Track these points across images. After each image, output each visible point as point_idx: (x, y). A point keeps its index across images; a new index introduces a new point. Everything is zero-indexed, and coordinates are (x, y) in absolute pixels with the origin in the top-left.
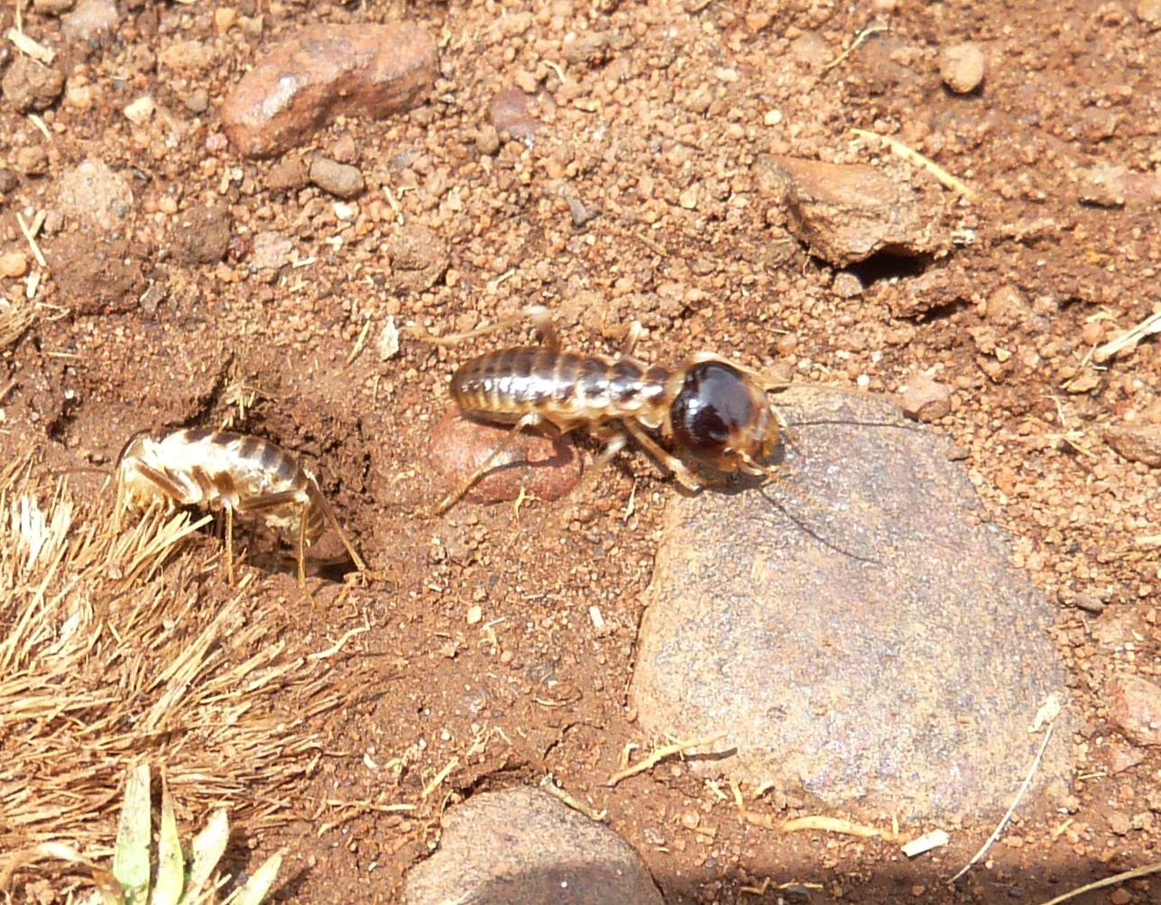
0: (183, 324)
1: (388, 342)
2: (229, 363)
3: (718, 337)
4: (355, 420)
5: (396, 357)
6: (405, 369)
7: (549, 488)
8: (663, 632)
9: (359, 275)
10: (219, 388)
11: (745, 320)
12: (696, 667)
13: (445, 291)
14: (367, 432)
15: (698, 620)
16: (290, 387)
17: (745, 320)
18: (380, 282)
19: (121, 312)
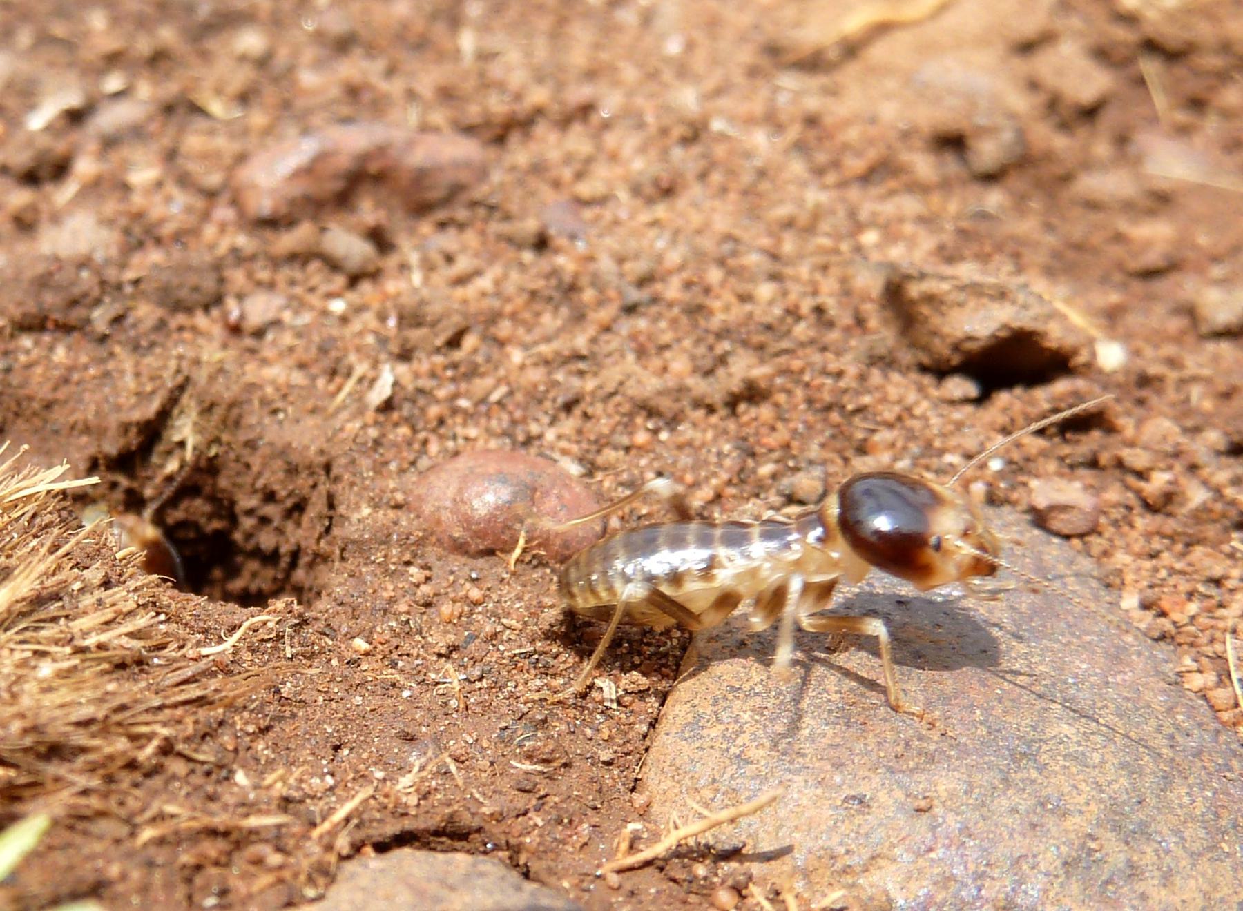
0: (136, 347)
1: (381, 392)
2: (181, 388)
3: (792, 425)
4: (322, 459)
5: (388, 406)
6: (396, 425)
7: (558, 542)
8: (696, 702)
9: (361, 334)
10: (164, 415)
11: (828, 408)
12: (739, 741)
13: (458, 355)
14: (335, 471)
15: (747, 687)
16: (251, 427)
17: (828, 408)
18: (383, 341)
19: (66, 329)
